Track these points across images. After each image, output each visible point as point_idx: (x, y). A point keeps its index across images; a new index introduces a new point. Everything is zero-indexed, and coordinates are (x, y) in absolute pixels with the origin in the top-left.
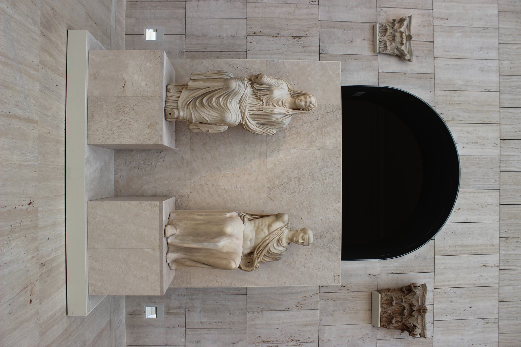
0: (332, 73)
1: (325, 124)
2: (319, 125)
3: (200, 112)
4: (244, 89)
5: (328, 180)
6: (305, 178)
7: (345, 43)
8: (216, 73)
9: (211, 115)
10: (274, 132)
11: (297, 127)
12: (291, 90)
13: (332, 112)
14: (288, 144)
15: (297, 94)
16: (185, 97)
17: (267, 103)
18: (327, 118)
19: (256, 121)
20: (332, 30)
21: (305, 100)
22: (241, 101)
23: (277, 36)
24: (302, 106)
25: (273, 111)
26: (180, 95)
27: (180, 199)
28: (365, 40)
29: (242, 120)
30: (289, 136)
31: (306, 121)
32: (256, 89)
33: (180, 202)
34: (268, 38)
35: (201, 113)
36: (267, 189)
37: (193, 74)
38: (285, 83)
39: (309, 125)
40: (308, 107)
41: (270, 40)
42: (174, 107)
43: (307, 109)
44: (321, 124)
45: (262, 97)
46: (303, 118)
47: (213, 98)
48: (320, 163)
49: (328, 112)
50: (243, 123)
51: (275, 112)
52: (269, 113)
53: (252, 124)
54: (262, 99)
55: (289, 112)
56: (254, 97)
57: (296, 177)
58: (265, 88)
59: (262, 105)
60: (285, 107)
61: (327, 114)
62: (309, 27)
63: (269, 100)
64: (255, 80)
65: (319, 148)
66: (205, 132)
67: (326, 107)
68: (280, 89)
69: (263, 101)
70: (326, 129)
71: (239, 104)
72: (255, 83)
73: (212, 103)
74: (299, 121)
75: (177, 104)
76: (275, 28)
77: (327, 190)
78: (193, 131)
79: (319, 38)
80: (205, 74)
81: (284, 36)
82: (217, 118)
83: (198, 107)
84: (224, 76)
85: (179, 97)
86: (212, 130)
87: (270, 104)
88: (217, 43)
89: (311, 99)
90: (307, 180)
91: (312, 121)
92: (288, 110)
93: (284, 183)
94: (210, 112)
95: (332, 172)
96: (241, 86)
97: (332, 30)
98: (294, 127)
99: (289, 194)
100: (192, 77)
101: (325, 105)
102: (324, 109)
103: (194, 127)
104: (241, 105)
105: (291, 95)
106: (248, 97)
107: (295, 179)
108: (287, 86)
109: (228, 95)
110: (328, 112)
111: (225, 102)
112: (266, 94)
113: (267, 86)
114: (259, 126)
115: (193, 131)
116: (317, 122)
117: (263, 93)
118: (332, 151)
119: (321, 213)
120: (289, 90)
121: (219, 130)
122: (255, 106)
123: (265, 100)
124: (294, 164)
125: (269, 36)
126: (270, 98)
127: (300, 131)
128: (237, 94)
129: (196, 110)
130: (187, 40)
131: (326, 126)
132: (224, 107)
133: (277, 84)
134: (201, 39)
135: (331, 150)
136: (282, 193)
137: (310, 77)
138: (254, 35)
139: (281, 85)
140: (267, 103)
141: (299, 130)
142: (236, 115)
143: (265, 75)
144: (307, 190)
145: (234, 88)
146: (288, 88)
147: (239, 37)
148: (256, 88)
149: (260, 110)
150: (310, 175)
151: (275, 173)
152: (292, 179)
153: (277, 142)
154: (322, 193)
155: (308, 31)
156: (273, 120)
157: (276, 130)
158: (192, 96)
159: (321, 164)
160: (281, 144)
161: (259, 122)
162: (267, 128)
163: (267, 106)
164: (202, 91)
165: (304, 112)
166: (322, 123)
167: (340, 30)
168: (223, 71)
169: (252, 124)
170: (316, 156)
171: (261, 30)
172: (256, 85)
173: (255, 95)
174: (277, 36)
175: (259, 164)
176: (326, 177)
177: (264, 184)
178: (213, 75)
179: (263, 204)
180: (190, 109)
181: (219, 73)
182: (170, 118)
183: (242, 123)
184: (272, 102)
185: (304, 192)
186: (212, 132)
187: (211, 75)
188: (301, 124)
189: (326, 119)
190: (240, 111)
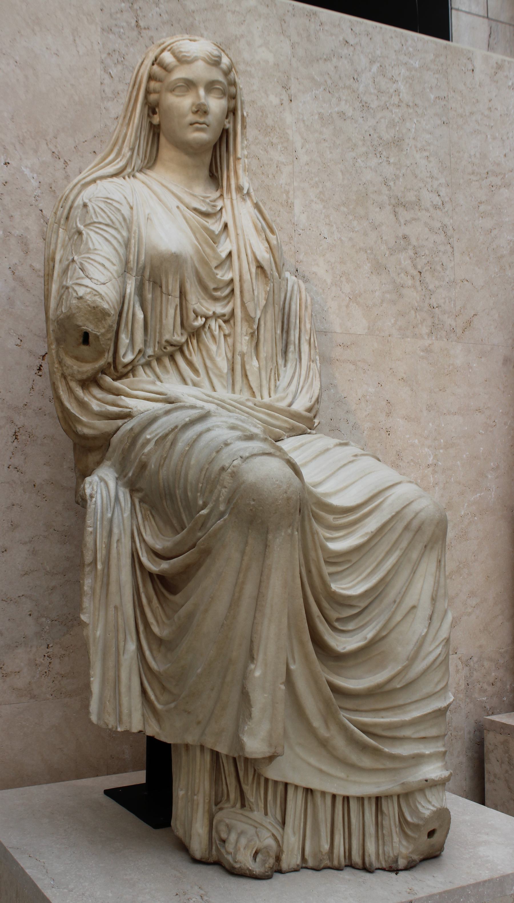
3: (420, 666)
5: (402, 87)
6: (397, 177)
13: (136, 6)
16: (312, 761)
17: (218, 294)
21: (202, 92)
25: (260, 267)
26: (296, 787)
27: (476, 695)
33: (485, 691)
36: (437, 339)
45: (192, 315)
48: (344, 107)
49: (138, 26)
54: (200, 322)
56: (190, 364)
57: (395, 213)
58: (137, 298)
61: (144, 33)
65: (286, 98)
67: (114, 29)
75: (361, 799)
77: (432, 97)
84: (116, 530)
85: (309, 791)
89: (201, 54)
90: (403, 171)
92: (239, 189)
93: (415, 266)
95: (372, 62)
99: (451, 250)
100: (130, 723)
101: (103, 30)
102: (120, 37)
106: (213, 394)
107: (402, 221)
108: (110, 179)
110: (138, 26)
112: (178, 294)
113: (131, 287)
118: (298, 43)
119: (505, 137)
120: (129, 170)
124: (351, 217)
133: (116, 229)
135: (293, 46)
136: (447, 280)
139: (119, 210)
140: (218, 294)
143: (81, 294)
144: (437, 179)
150: (384, 153)
151: (383, 301)
152: (400, 235)
154: (444, 119)
158: (317, 723)
159: (346, 101)
170: (317, 117)
172: (122, 351)
173: (172, 357)
175: (353, 367)
176: (392, 91)
177: (423, 351)
178: (114, 600)
179: (483, 359)
180: (403, 725)
181: (99, 566)
184: (214, 264)
185: (443, 192)
187: (116, 608)
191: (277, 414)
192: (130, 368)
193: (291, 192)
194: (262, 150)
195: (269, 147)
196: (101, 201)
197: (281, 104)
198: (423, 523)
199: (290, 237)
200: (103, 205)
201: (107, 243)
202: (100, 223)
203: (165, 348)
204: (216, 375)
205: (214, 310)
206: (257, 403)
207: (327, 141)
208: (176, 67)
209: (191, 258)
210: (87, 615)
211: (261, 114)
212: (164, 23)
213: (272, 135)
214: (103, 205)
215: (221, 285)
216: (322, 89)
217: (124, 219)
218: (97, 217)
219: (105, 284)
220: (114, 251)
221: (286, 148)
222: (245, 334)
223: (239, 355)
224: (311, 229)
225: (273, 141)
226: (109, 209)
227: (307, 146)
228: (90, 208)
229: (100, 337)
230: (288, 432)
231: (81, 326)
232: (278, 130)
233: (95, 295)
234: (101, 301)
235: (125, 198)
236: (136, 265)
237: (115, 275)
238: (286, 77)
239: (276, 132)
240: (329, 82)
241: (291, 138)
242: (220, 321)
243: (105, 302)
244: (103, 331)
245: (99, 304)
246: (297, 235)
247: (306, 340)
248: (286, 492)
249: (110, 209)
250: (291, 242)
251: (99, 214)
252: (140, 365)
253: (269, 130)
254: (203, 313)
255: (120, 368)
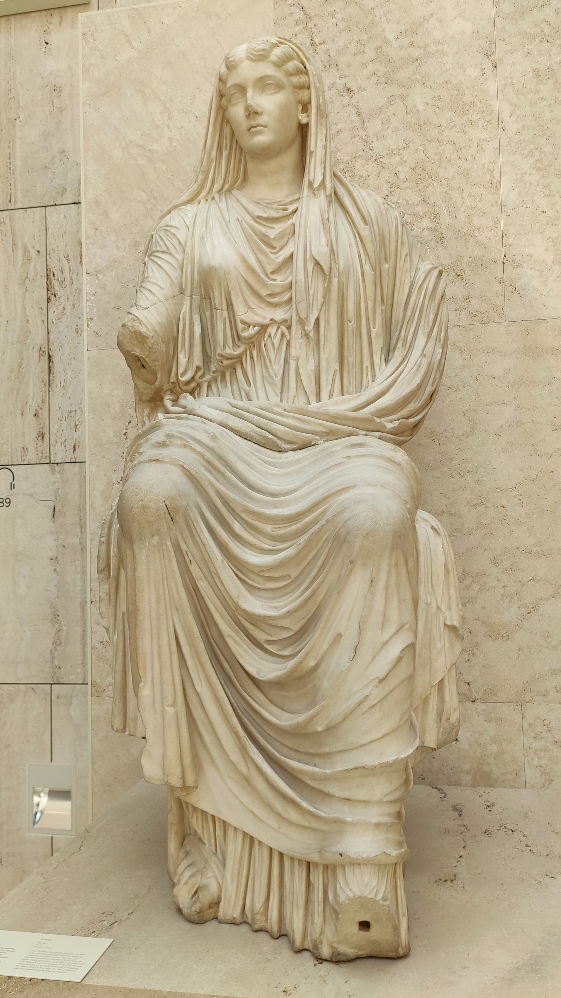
0: (133, 48)
1: (367, 50)
2: (374, 79)
4: (195, 422)
7: (61, 110)
8: (113, 590)
9: (361, 630)
10: (431, 270)
11: (387, 182)
12: (202, 187)
13: (310, 25)
14: (476, 221)
15: (225, 153)
17: (275, 300)
18: (341, 43)
19: (377, 360)
20: (19, 163)
22: (266, 438)
23: (50, 357)
24: (284, 109)
25: (317, 263)
28: (47, 43)
29: (378, 434)
30: (435, 217)
31: (360, 145)
32: (201, 365)
34: (56, 389)
35: (356, 699)
37: (118, 723)
38: (167, 217)
39: (375, 126)
40: (289, 74)
41: (63, 383)
42: (318, 895)
43: (296, 80)
44: (371, 67)
45: (240, 326)
46: (346, 158)
47: (244, 611)
50: (389, 426)
51: (326, 250)
52: (330, 282)
53: (395, 381)
54: (252, 331)
55: (319, 178)
58: (196, 317)
59: (289, 328)
60: (291, 208)
62: (14, 245)
63: (264, 292)
64: (155, 374)
65: (488, 65)
66: (458, 648)
68: (197, 238)
69: (267, 321)
70: (395, 44)
71: (281, 451)
72: (173, 374)
73: (282, 617)
74: (361, 176)
76: (20, 365)
78: (453, 719)
79: (47, 208)
80: (121, 654)
81: (48, 333)
82: (382, 583)
83: (310, 720)
86: (444, 609)
87: (280, 280)
88: (79, 569)
91: (359, 114)
92: (311, 184)
94: (340, 635)
96: (168, 436)
97: (19, 163)
98: (391, 197)
103: (432, 716)
104: (287, 438)
105: (229, 190)
108: (182, 207)
109: (223, 510)
111: (268, 528)
112: (225, 307)
113: (186, 308)
114: (404, 344)
115: (453, 719)
116: (360, 89)
117: (220, 326)
120: (204, 193)
121: (446, 565)
122: (293, 364)
123: (260, 311)
125: (49, 386)
126: (247, 282)
127: (408, 169)
128: (221, 458)
129: (331, 729)
130: (71, 677)
131: (378, 43)
132: (303, 539)
134: (65, 628)
137: (155, 147)
138: (46, 436)
139: (174, 235)
140: (275, 300)
141: (404, 172)
142: (349, 457)
145: (177, 475)
146: (190, 201)
147: (57, 491)
148: (198, 368)
149: (312, 334)
153: (466, 277)
155: (25, 249)
156: (367, 267)
157: (415, 258)
160: (477, 252)
161: (378, 345)
162: (407, 303)
163: (290, 299)
164: (202, 688)
165: (318, 99)
166: (364, 65)
167: (19, 134)
168: (104, 547)
169: (395, 381)
170: (530, 75)
171: (29, 415)
172: (181, 370)
174: (50, 357)
182: (396, 929)
183: (394, 432)
184: (269, 269)
186: (454, 608)
187: (123, 614)
188: (372, 167)
189: (346, 47)
190: (323, 445)
191: (307, 418)
192: (193, 385)
193: (497, 170)
194: (458, 132)
195: (466, 126)
196: (162, 229)
197: (483, 75)
198: (348, 533)
199: (496, 220)
200: (162, 234)
201: (160, 269)
202: (157, 251)
203: (222, 362)
204: (270, 383)
205: (272, 318)
206: (287, 408)
207: (545, 99)
208: (228, 75)
209: (236, 268)
210: (106, 619)
211: (456, 92)
212: (340, 32)
213: (471, 112)
214: (162, 234)
215: (277, 290)
216: (537, 41)
217: (180, 243)
218: (156, 246)
219: (147, 309)
220: (165, 276)
221: (490, 122)
222: (300, 337)
223: (292, 360)
224: (525, 206)
225: (472, 120)
226: (166, 236)
227: (518, 112)
228: (154, 237)
229: (147, 359)
230: (325, 436)
231: (131, 352)
232: (478, 104)
233: (134, 320)
234: (139, 325)
235: (185, 221)
236: (189, 285)
237: (162, 298)
238: (488, 42)
239: (475, 108)
240: (547, 30)
241: (496, 109)
242: (283, 328)
243: (143, 325)
244: (147, 353)
245: (136, 328)
246: (504, 217)
247: (423, 333)
248: (142, 500)
249: (168, 236)
250: (497, 225)
251: (158, 242)
252: (206, 381)
253: (467, 107)
254: (254, 322)
255: (181, 386)
